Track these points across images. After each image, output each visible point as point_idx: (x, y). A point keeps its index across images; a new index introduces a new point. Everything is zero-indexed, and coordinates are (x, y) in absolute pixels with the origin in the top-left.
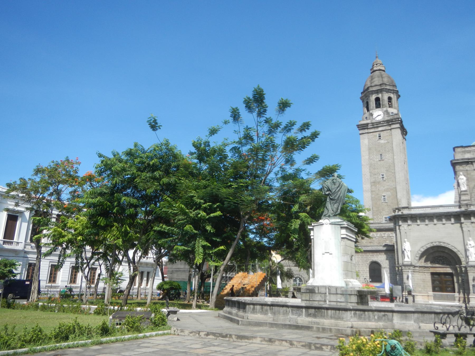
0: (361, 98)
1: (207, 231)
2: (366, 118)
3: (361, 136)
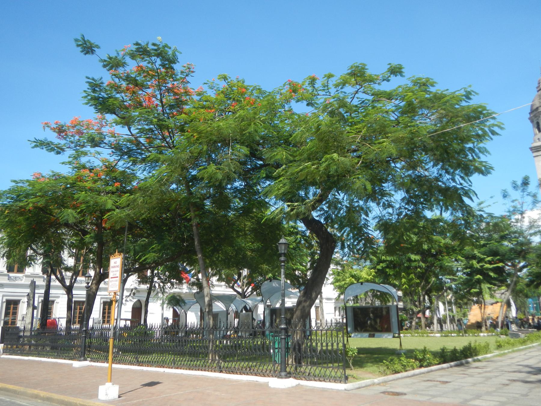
0: (530, 119)
1: (491, 276)
2: (539, 139)
3: (536, 158)
